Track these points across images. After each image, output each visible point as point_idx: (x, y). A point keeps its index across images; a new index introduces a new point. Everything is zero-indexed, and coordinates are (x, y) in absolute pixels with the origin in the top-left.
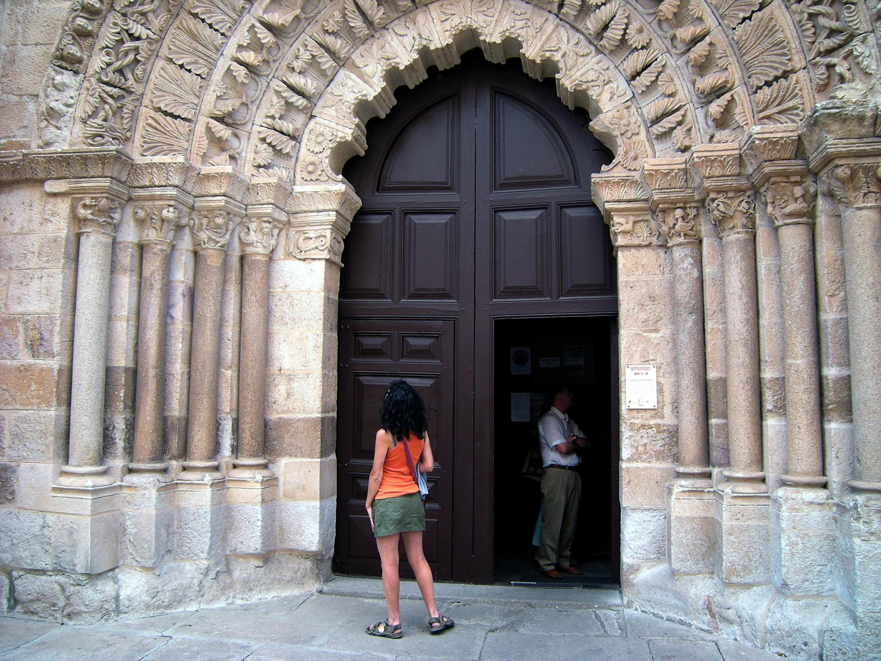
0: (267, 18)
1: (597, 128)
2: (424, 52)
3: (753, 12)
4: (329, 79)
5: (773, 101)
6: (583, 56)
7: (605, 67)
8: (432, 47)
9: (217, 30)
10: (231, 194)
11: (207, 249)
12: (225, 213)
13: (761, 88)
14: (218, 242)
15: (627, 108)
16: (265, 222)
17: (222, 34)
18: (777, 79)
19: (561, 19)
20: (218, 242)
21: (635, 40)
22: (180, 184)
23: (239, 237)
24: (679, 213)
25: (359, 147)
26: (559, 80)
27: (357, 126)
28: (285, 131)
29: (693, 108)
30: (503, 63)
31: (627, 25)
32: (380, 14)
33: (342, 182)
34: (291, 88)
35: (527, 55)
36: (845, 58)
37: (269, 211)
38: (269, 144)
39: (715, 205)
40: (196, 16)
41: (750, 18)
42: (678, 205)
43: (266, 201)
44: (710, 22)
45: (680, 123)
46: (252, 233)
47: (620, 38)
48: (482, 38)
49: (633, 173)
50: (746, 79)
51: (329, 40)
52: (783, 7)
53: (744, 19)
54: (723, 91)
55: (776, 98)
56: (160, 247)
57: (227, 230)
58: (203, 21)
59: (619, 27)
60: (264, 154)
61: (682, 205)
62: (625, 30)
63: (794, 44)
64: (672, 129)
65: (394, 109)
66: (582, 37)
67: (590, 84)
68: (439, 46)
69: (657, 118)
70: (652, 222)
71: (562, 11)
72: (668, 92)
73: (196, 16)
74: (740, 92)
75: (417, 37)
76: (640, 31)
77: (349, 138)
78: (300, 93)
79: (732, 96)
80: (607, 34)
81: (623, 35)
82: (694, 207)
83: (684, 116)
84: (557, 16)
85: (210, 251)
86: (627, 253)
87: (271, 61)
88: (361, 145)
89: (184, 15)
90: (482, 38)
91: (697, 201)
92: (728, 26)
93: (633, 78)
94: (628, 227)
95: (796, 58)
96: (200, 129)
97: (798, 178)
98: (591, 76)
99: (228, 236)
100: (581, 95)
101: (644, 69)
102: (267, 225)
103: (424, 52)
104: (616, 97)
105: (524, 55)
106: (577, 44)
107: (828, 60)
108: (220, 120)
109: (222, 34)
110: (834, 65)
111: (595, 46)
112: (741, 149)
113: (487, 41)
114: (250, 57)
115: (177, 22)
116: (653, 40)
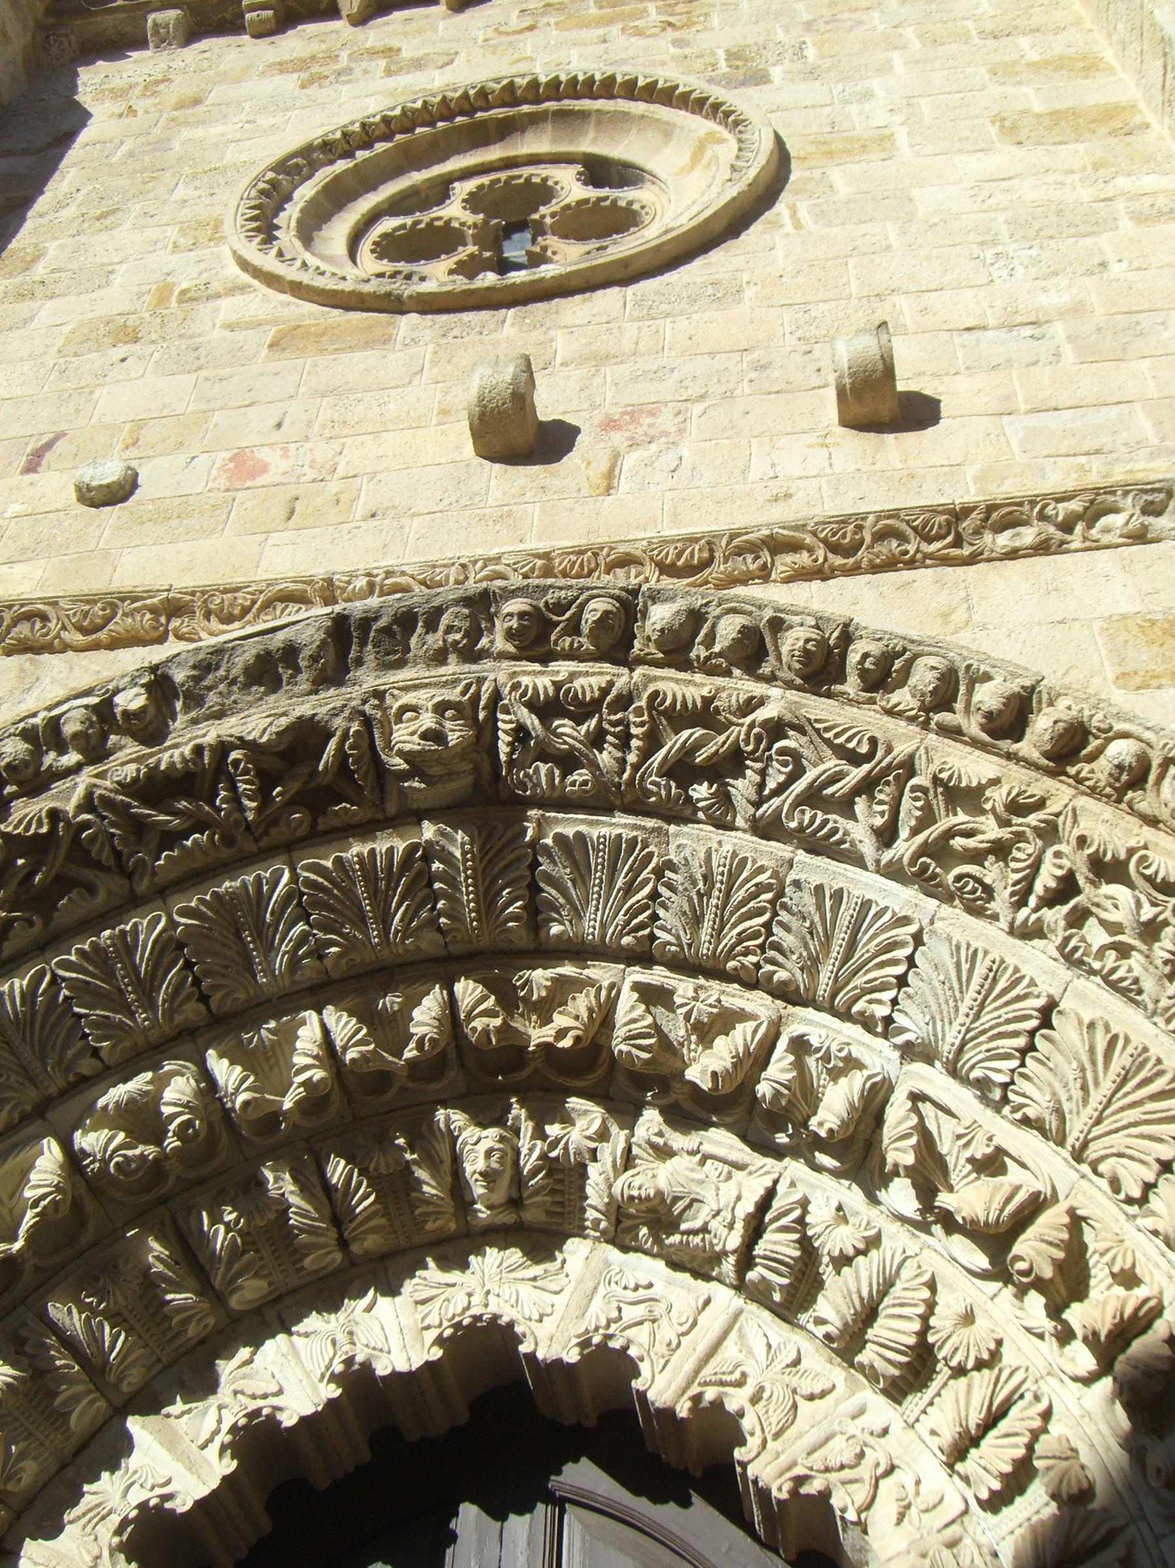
6: (811, 1398)
7: (878, 1429)
15: (952, 1544)
21: (953, 1343)
26: (744, 1465)
31: (931, 1305)
35: (651, 1395)
47: (912, 1341)
48: (524, 1348)
62: (925, 1318)
67: (834, 1477)
76: (968, 1318)
80: (878, 1330)
81: (922, 1334)
90: (524, 1348)
98: (839, 1451)
104: (913, 1511)
105: (642, 1395)
106: (797, 1362)
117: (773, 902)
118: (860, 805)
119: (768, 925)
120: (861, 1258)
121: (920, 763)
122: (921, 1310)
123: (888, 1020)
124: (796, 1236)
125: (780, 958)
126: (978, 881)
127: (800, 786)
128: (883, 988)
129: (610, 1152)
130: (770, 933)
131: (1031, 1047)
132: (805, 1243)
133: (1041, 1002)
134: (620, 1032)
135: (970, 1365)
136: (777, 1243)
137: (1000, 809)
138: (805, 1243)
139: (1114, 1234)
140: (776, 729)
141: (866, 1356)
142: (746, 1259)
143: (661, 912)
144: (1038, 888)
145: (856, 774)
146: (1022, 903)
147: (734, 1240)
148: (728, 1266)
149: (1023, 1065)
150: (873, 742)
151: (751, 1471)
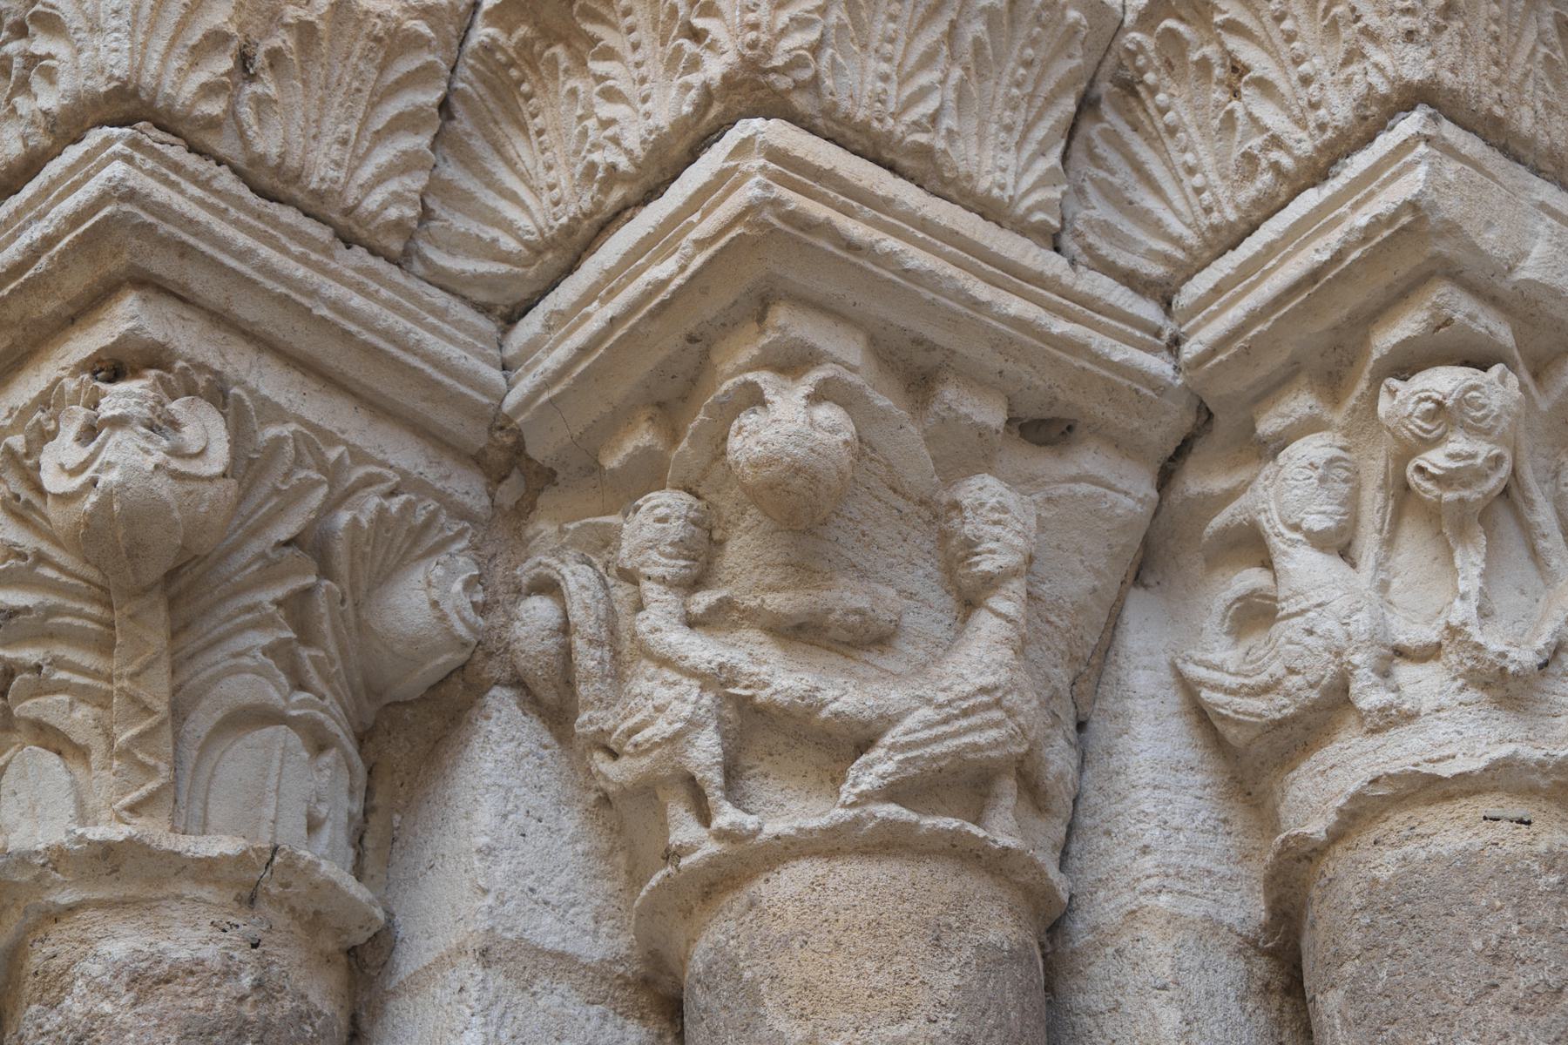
10: (858, 84)
11: (744, 863)
12: (846, 351)
14: (858, 739)
16: (1406, 364)
20: (858, 739)
22: (185, 86)
23: (1188, 688)
37: (1410, 185)
43: (1340, 109)
46: (1305, 567)
56: (121, 943)
57: (969, 603)
85: (787, 885)
99: (982, 656)
102: (1444, 381)
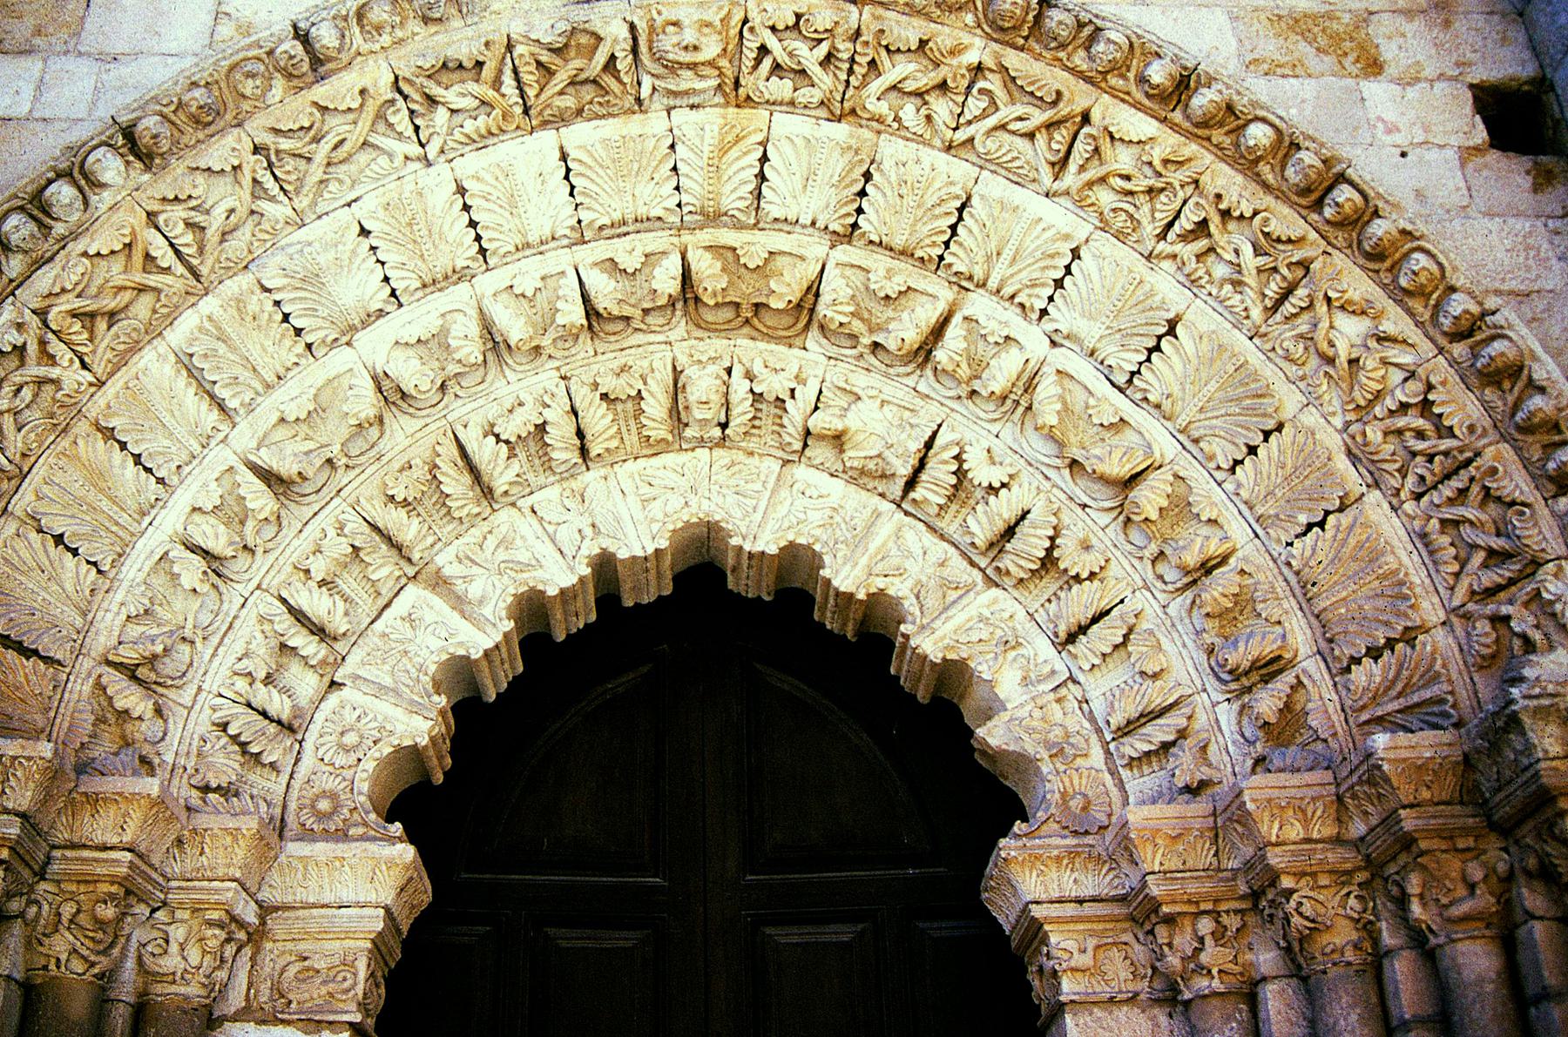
0: (266, 459)
1: (990, 741)
2: (605, 565)
3: (1327, 513)
4: (381, 602)
5: (1389, 688)
8: (623, 554)
9: (148, 470)
13: (1358, 661)
17: (160, 481)
18: (1390, 644)
19: (907, 513)
21: (1071, 558)
24: (1206, 926)
25: (435, 761)
26: (906, 637)
27: (442, 713)
28: (272, 712)
29: (1207, 703)
30: (767, 598)
32: (510, 475)
33: (401, 840)
34: (298, 615)
36: (1526, 605)
38: (235, 739)
39: (1293, 904)
40: (108, 433)
41: (1321, 524)
42: (1203, 907)
44: (1238, 531)
45: (1182, 734)
49: (1089, 840)
50: (1323, 645)
51: (393, 519)
52: (1386, 506)
53: (1310, 527)
54: (1275, 667)
55: (1393, 682)
58: (123, 446)
59: (1039, 532)
60: (220, 759)
61: (1209, 906)
63: (1418, 577)
64: (1166, 747)
65: (515, 683)
66: (952, 550)
68: (640, 553)
69: (1129, 722)
70: (1137, 947)
71: (912, 495)
72: (1151, 668)
73: (108, 433)
74: (1312, 670)
75: (588, 531)
77: (423, 741)
78: (319, 631)
79: (1297, 677)
81: (1049, 551)
82: (1236, 912)
83: (1189, 718)
84: (899, 506)
86: (1086, 1018)
87: (260, 550)
88: (440, 758)
89: (82, 427)
90: (734, 541)
91: (1242, 898)
92: (1279, 541)
93: (1071, 638)
94: (1085, 960)
95: (1425, 605)
96: (81, 688)
97: (1471, 842)
100: (952, 675)
101: (1095, 620)
103: (605, 565)
105: (828, 582)
107: (1490, 609)
108: (130, 672)
109: (160, 481)
110: (1507, 618)
111: (983, 571)
112: (1338, 785)
113: (747, 547)
114: (215, 537)
115: (65, 443)
116: (1113, 562)
117: (961, 210)
118: (1041, 138)
119: (953, 228)
120: (1003, 491)
121: (1095, 115)
122: (1051, 532)
123: (1044, 312)
124: (954, 468)
125: (960, 252)
126: (1131, 216)
127: (991, 122)
128: (1043, 285)
129: (807, 394)
130: (954, 232)
131: (1157, 348)
132: (960, 473)
133: (1171, 315)
134: (825, 298)
135: (1085, 575)
136: (940, 472)
137: (1157, 163)
138: (960, 473)
139: (1208, 494)
140: (979, 69)
141: (1006, 562)
142: (911, 484)
143: (865, 205)
144: (1177, 228)
145: (1039, 117)
146: (1162, 236)
147: (904, 470)
148: (896, 489)
149: (1148, 360)
150: (1059, 94)
151: (913, 643)
